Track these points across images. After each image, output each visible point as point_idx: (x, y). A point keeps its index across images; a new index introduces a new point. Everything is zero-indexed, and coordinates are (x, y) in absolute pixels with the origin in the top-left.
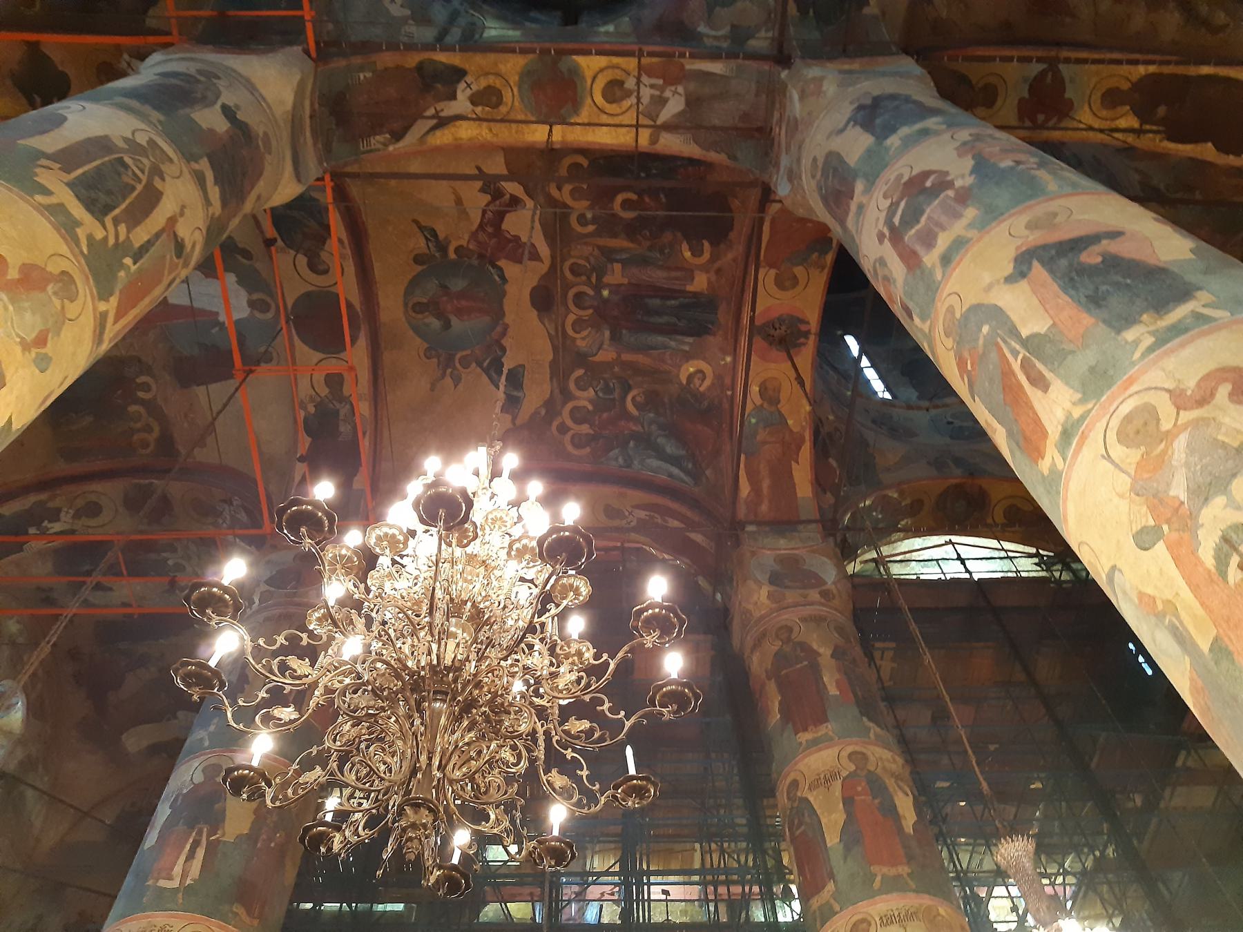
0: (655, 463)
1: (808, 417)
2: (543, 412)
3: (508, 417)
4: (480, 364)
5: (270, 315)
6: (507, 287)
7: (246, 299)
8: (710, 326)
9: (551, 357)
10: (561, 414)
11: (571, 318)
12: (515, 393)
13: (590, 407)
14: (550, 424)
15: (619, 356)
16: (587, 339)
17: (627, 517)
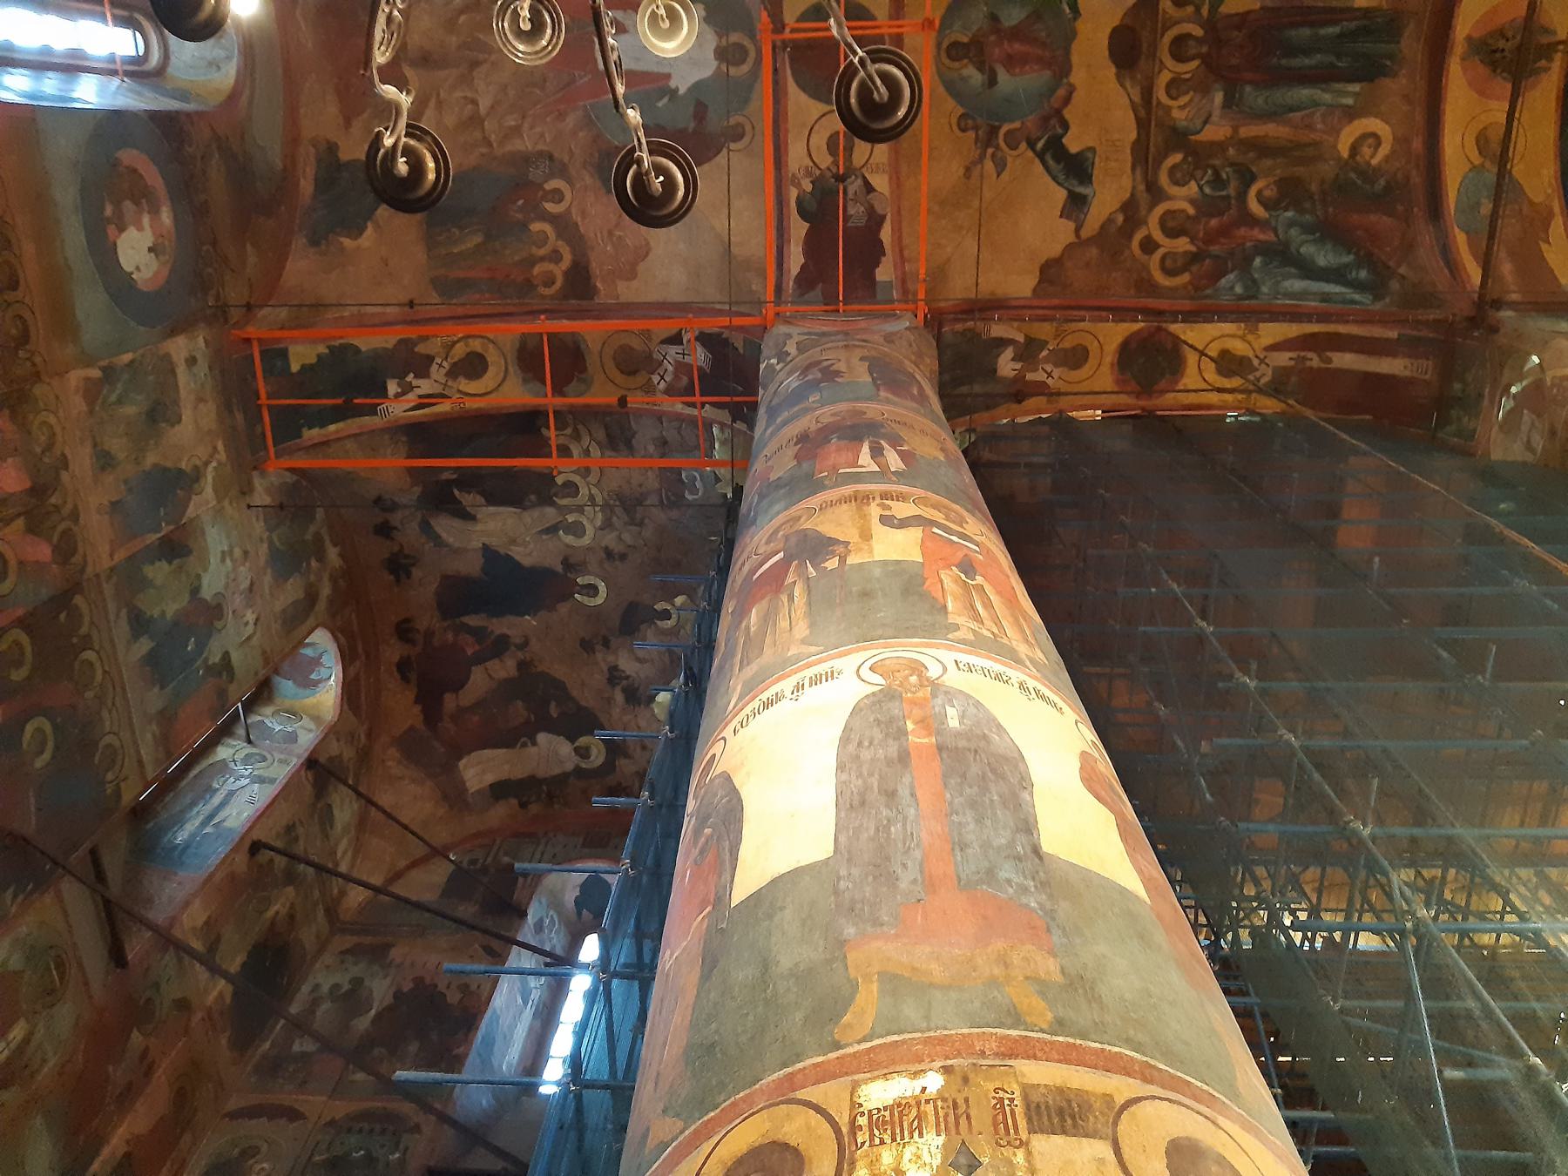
0: (1298, 285)
1: (1554, 182)
2: (1120, 218)
3: (1071, 225)
4: (1031, 145)
5: (745, 68)
6: (1080, 25)
7: (713, 45)
8: (1388, 63)
9: (1133, 135)
10: (1146, 223)
11: (1164, 78)
12: (1081, 190)
13: (1191, 211)
14: (1130, 237)
15: (1235, 129)
16: (1187, 110)
17: (1257, 370)
